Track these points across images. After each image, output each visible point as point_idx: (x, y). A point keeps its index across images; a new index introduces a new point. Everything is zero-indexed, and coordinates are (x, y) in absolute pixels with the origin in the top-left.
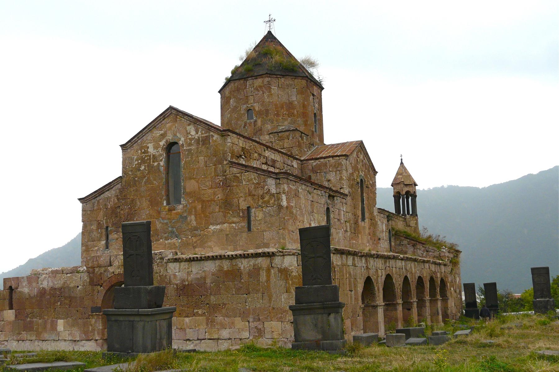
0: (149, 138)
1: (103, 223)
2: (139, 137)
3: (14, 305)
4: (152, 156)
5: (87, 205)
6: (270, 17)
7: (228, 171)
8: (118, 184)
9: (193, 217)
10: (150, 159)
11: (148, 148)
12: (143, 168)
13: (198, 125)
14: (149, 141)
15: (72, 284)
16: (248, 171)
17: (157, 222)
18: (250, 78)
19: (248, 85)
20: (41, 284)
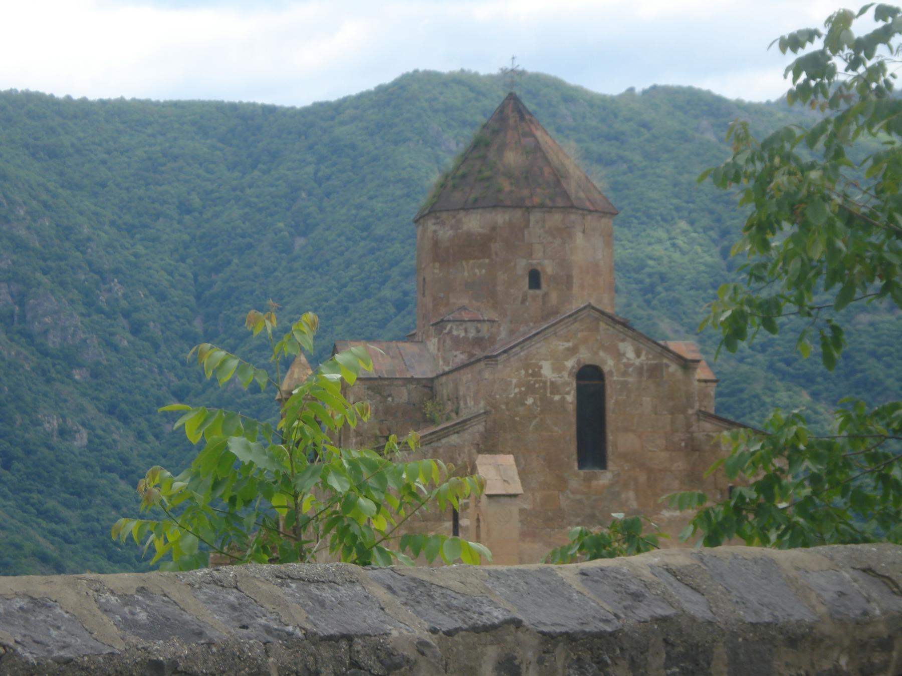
4: (548, 383)
7: (694, 428)
9: (631, 494)
10: (545, 388)
12: (530, 401)
13: (641, 343)
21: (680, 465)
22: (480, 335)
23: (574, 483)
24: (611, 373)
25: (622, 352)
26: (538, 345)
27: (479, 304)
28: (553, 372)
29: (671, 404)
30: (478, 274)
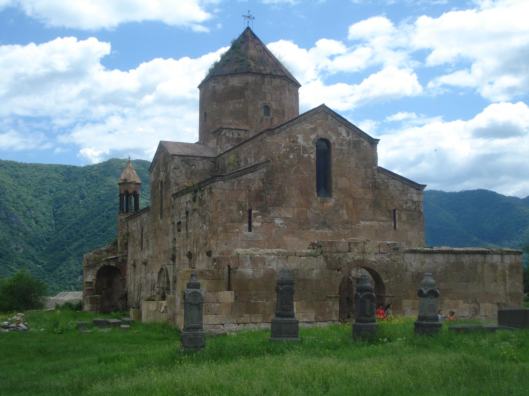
0: (299, 128)
1: (246, 205)
2: (289, 125)
3: (233, 286)
4: (301, 147)
5: (226, 184)
6: (249, 14)
7: (376, 177)
8: (264, 167)
9: (345, 211)
10: (299, 150)
11: (298, 138)
12: (291, 156)
13: (350, 128)
14: (298, 132)
15: (307, 267)
16: (394, 179)
17: (308, 211)
18: (268, 76)
19: (266, 82)
20: (270, 265)
21: (369, 196)
22: (240, 137)
23: (315, 204)
24: (334, 143)
25: (340, 132)
26: (296, 125)
27: (238, 122)
28: (304, 141)
29: (365, 163)
30: (238, 107)
